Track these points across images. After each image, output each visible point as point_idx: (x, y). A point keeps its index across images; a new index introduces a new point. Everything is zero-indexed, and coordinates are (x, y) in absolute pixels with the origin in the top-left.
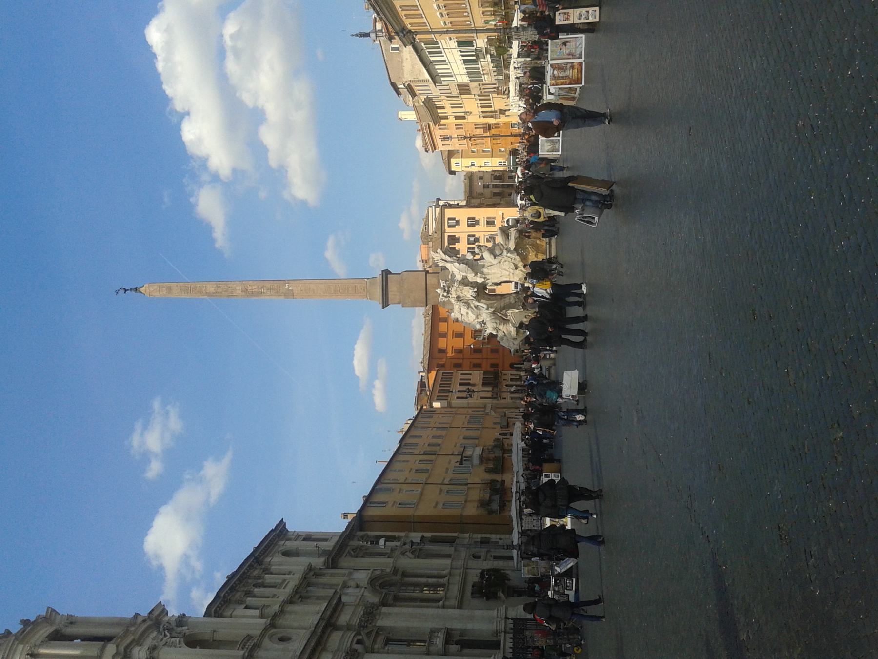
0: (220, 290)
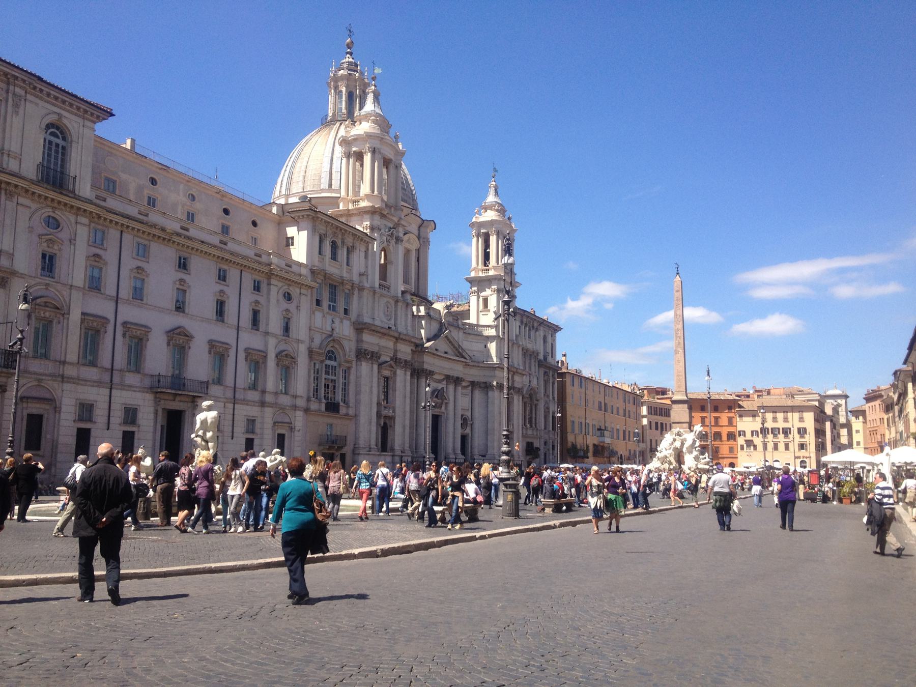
0: (678, 317)
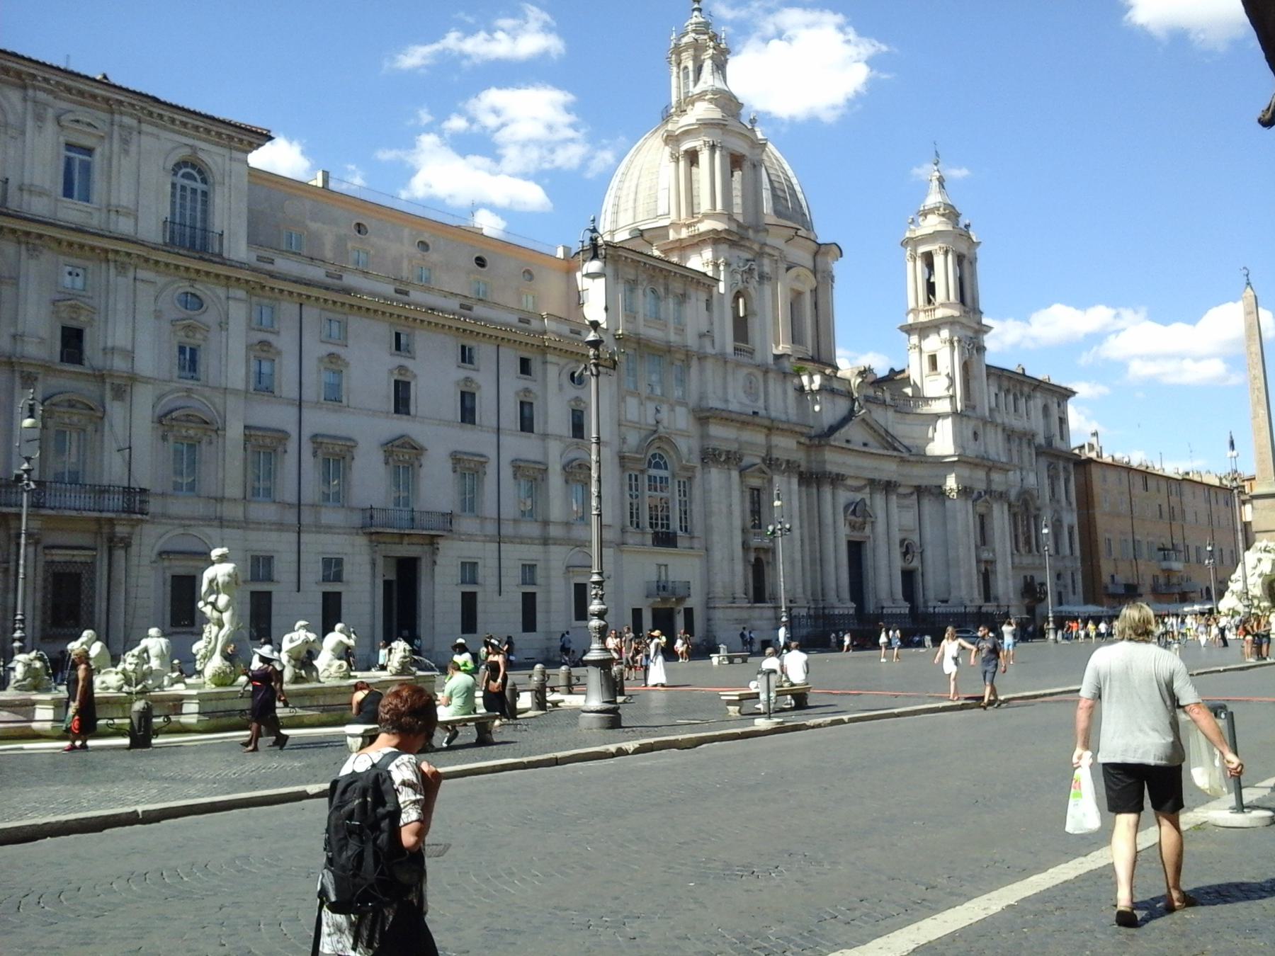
0: (1253, 355)
